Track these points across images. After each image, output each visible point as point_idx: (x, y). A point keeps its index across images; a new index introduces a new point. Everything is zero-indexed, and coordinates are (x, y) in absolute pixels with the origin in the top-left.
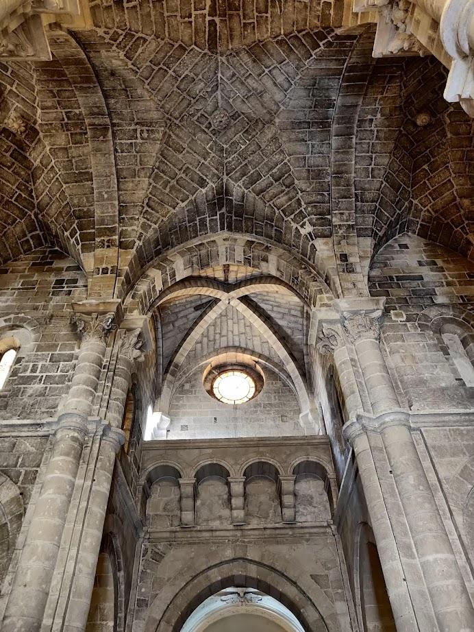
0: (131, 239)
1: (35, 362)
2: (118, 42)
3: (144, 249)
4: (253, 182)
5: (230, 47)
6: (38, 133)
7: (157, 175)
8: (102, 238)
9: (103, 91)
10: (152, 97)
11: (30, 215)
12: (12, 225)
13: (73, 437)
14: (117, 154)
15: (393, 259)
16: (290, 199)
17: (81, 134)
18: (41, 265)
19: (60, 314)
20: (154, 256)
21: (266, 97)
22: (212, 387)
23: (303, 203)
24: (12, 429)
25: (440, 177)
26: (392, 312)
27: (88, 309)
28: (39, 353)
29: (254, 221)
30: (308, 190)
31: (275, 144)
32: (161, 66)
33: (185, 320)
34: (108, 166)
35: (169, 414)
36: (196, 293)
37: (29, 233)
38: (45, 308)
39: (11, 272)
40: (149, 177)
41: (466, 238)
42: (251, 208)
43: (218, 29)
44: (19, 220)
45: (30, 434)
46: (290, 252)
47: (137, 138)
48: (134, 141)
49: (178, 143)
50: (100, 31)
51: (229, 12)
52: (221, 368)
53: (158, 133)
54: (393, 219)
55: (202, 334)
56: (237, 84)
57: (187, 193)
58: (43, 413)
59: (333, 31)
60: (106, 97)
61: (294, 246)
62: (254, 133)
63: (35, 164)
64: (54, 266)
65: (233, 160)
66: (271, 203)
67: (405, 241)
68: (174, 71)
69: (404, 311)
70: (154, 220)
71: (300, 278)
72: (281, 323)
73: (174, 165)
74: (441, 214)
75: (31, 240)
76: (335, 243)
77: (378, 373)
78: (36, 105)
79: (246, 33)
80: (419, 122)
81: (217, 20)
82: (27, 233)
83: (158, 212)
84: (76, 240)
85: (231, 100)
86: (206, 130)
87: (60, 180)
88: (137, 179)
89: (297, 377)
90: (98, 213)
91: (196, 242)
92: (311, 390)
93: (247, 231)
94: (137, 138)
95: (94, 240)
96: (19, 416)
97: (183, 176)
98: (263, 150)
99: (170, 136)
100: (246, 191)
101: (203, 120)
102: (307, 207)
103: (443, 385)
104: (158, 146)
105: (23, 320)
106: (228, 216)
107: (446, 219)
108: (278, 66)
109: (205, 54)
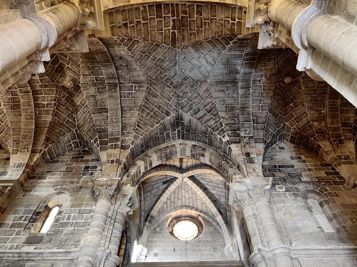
0: (127, 144)
1: (70, 214)
2: (124, 42)
3: (135, 150)
4: (196, 113)
5: (183, 44)
7: (143, 110)
9: (115, 67)
10: (141, 69)
11: (73, 131)
12: (63, 136)
13: (88, 260)
14: (122, 99)
15: (276, 155)
16: (216, 122)
17: (103, 88)
18: (77, 158)
19: (86, 186)
20: (140, 153)
21: (203, 69)
22: (172, 230)
23: (223, 124)
24: (52, 255)
25: (299, 111)
26: (277, 186)
27: (102, 183)
28: (72, 209)
29: (197, 134)
30: (226, 117)
32: (146, 54)
33: (157, 190)
34: (117, 105)
35: (147, 246)
36: (164, 174)
38: (78, 182)
39: (60, 162)
40: (139, 111)
41: (317, 144)
42: (195, 127)
43: (176, 36)
44: (67, 133)
45: (63, 258)
46: (217, 151)
48: (131, 92)
49: (155, 93)
50: (115, 38)
51: (182, 28)
52: (178, 219)
54: (275, 133)
55: (167, 198)
56: (187, 62)
57: (160, 119)
58: (72, 245)
59: (237, 36)
60: (117, 69)
61: (219, 148)
62: (196, 87)
63: (78, 104)
64: (84, 159)
65: (185, 102)
66: (206, 124)
67: (282, 145)
68: (153, 56)
69: (284, 185)
70: (141, 133)
71: (223, 166)
72: (213, 192)
73: (152, 104)
74: (302, 130)
75: (72, 144)
76: (242, 146)
77: (270, 223)
78: (80, 74)
79: (191, 37)
80: (286, 81)
81: (176, 31)
82: (71, 140)
83: (143, 129)
84: (97, 144)
85: (183, 71)
86: (170, 86)
87: (90, 112)
88: (132, 111)
89: (223, 224)
90: (110, 130)
91: (164, 145)
92: (231, 232)
93: (192, 140)
95: (107, 145)
96: (57, 247)
97: (157, 110)
98: (202, 96)
99: (150, 89)
100: (192, 118)
101: (168, 80)
102: (226, 127)
103: (310, 231)
104: (144, 94)
105: (65, 189)
106: (182, 132)
107: (305, 133)
108: (209, 53)
109: (170, 48)
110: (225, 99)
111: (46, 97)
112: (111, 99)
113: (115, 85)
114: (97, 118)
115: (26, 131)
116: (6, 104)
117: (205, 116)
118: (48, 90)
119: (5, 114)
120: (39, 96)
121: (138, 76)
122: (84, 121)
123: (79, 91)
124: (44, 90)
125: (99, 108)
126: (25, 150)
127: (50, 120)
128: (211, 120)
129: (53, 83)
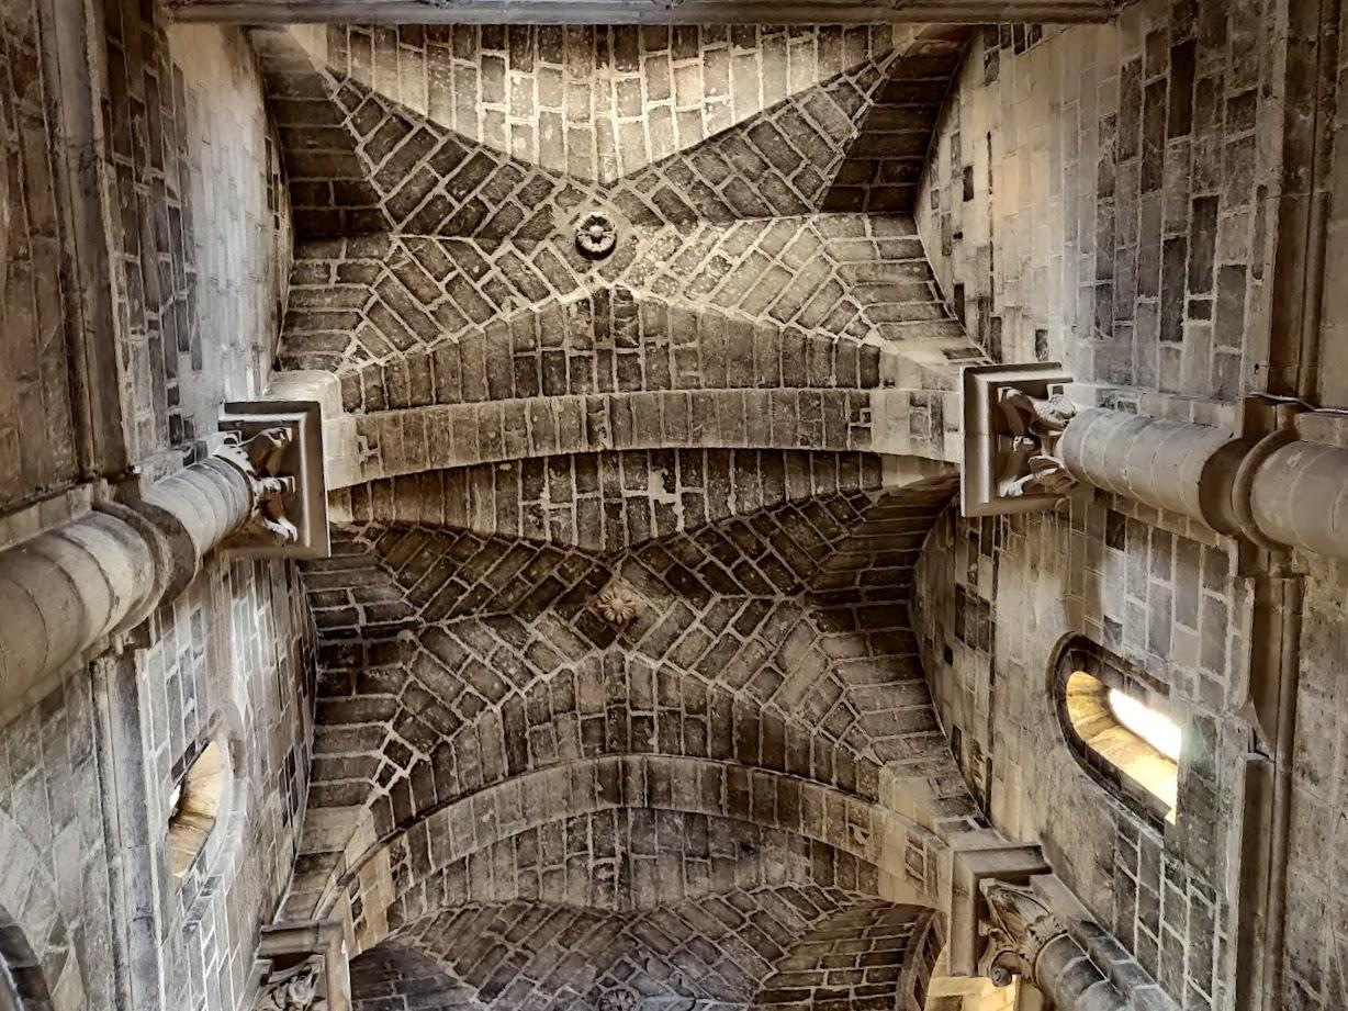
6: (602, 647)
8: (408, 850)
12: (399, 581)
17: (603, 739)
34: (543, 810)
37: (366, 609)
40: (520, 899)
47: (597, 857)
48: (591, 852)
53: (608, 900)
63: (530, 627)
68: (732, 937)
75: (343, 608)
78: (665, 660)
81: (809, 1001)
87: (508, 695)
88: (516, 873)
94: (597, 857)
97: (511, 954)
99: (599, 920)
101: (623, 971)
111: (566, 505)
112: (565, 784)
113: (618, 793)
114: (486, 735)
115: (435, 430)
116: (537, 325)
118: (596, 517)
119: (494, 312)
120: (574, 476)
121: (656, 883)
122: (462, 661)
123: (586, 640)
124: (598, 499)
125: (527, 735)
126: (367, 452)
127: (476, 527)
129: (626, 544)
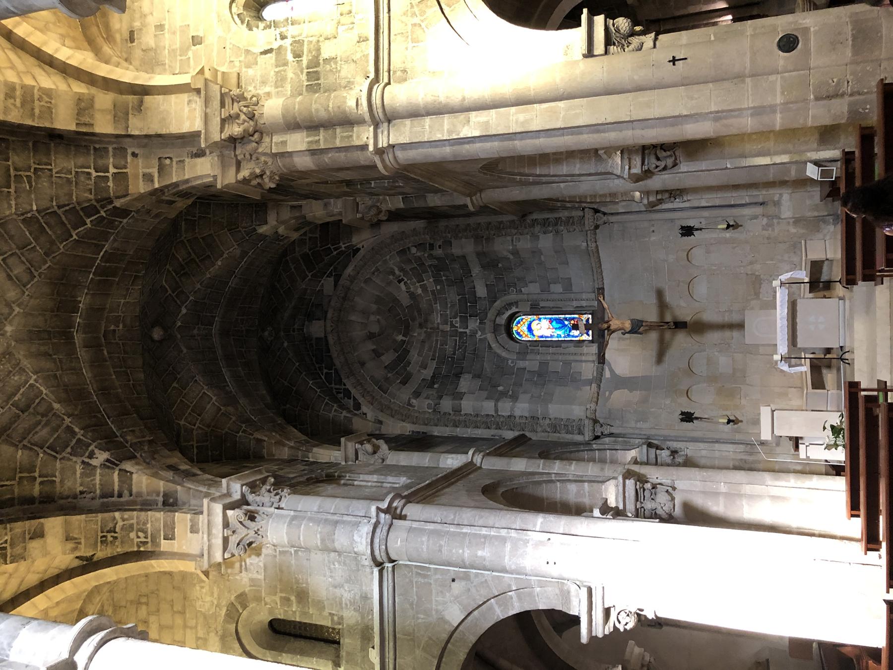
23: (77, 430)
30: (76, 413)
31: (9, 361)
59: (111, 202)
61: (82, 493)
66: (25, 442)
71: (120, 523)
110: (58, 373)
117: (15, 421)
128: (37, 429)
